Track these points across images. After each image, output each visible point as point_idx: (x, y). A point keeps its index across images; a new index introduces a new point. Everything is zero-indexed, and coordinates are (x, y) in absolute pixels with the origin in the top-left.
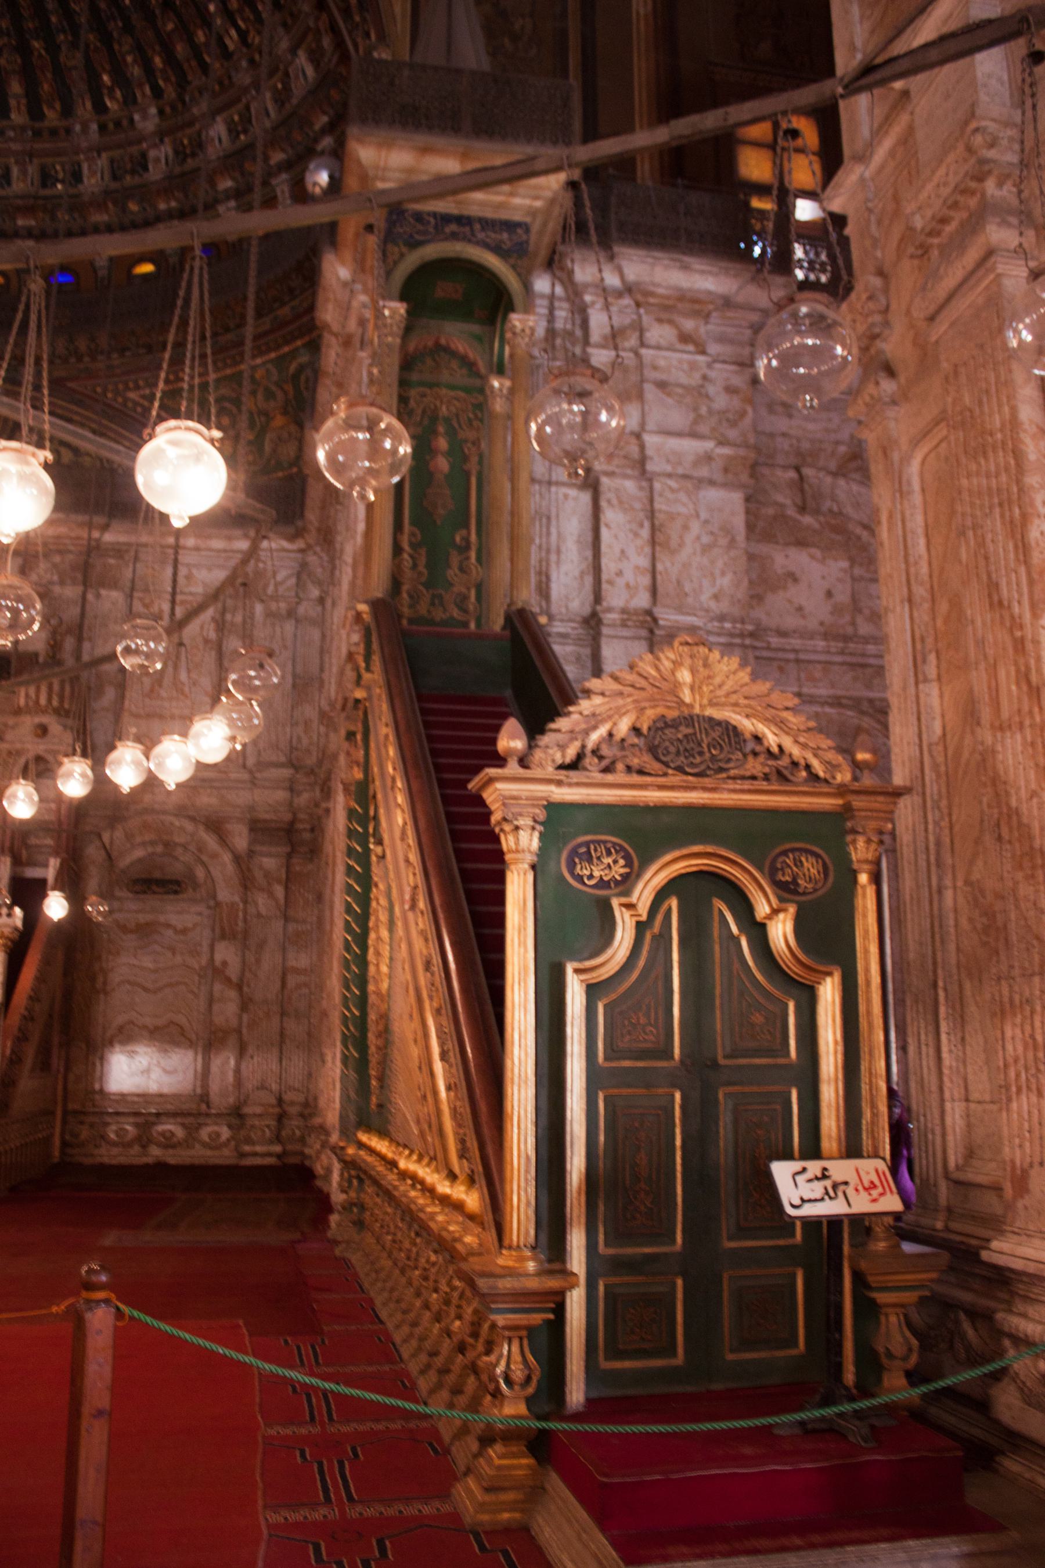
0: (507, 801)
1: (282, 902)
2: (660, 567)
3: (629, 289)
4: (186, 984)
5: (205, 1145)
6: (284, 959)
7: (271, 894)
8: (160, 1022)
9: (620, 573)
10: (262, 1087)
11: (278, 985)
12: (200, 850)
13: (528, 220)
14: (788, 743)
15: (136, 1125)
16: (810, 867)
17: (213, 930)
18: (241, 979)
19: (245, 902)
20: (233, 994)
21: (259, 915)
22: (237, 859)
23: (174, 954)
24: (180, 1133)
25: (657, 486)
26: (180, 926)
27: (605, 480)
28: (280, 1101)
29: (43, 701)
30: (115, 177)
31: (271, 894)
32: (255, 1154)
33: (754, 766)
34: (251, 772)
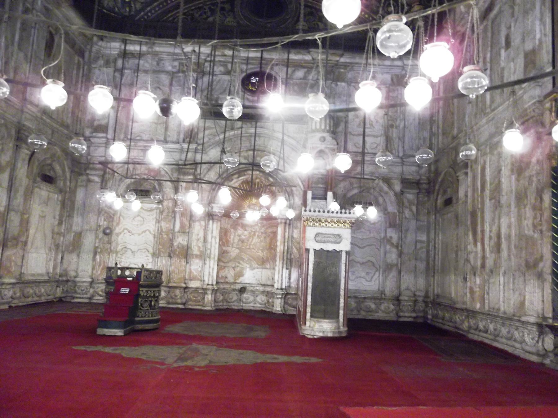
4: (375, 245)
5: (383, 312)
6: (416, 237)
8: (364, 261)
10: (407, 289)
11: (413, 248)
12: (380, 190)
15: (356, 302)
17: (386, 223)
18: (398, 244)
19: (399, 212)
20: (394, 250)
21: (406, 218)
22: (396, 195)
23: (370, 233)
28: (415, 295)
29: (323, 127)
31: (411, 210)
32: (405, 317)
34: (402, 158)
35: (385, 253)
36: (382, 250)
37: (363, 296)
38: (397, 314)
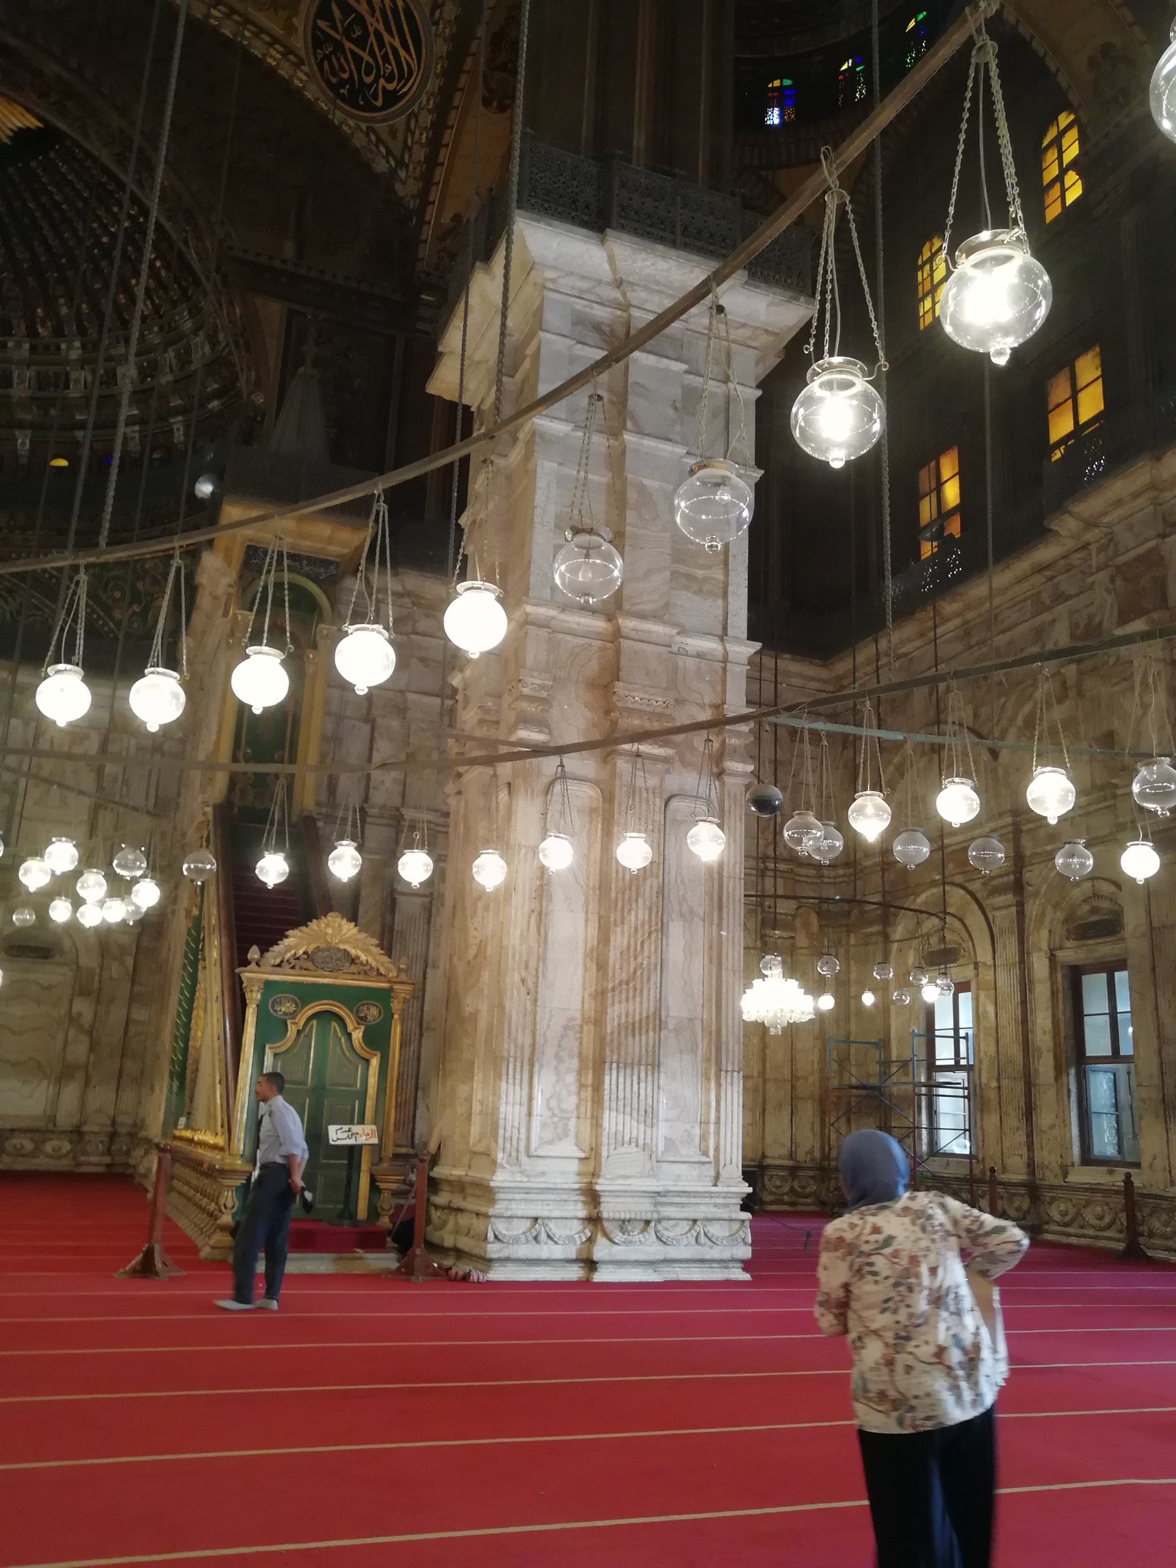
0: (249, 979)
1: (131, 967)
2: (408, 780)
3: (408, 594)
5: (48, 1156)
7: (122, 963)
9: (383, 783)
10: (99, 1111)
13: (339, 560)
14: (370, 960)
16: (374, 1011)
18: (92, 1027)
19: (102, 968)
20: (85, 1040)
21: (111, 978)
24: (29, 1146)
25: (413, 727)
26: (46, 984)
27: (379, 720)
28: (113, 1122)
30: (40, 388)
31: (122, 963)
32: (89, 1164)
33: (354, 969)
35: (66, 1042)
36: (60, 1038)
37: (9, 1126)
38: (74, 1158)
